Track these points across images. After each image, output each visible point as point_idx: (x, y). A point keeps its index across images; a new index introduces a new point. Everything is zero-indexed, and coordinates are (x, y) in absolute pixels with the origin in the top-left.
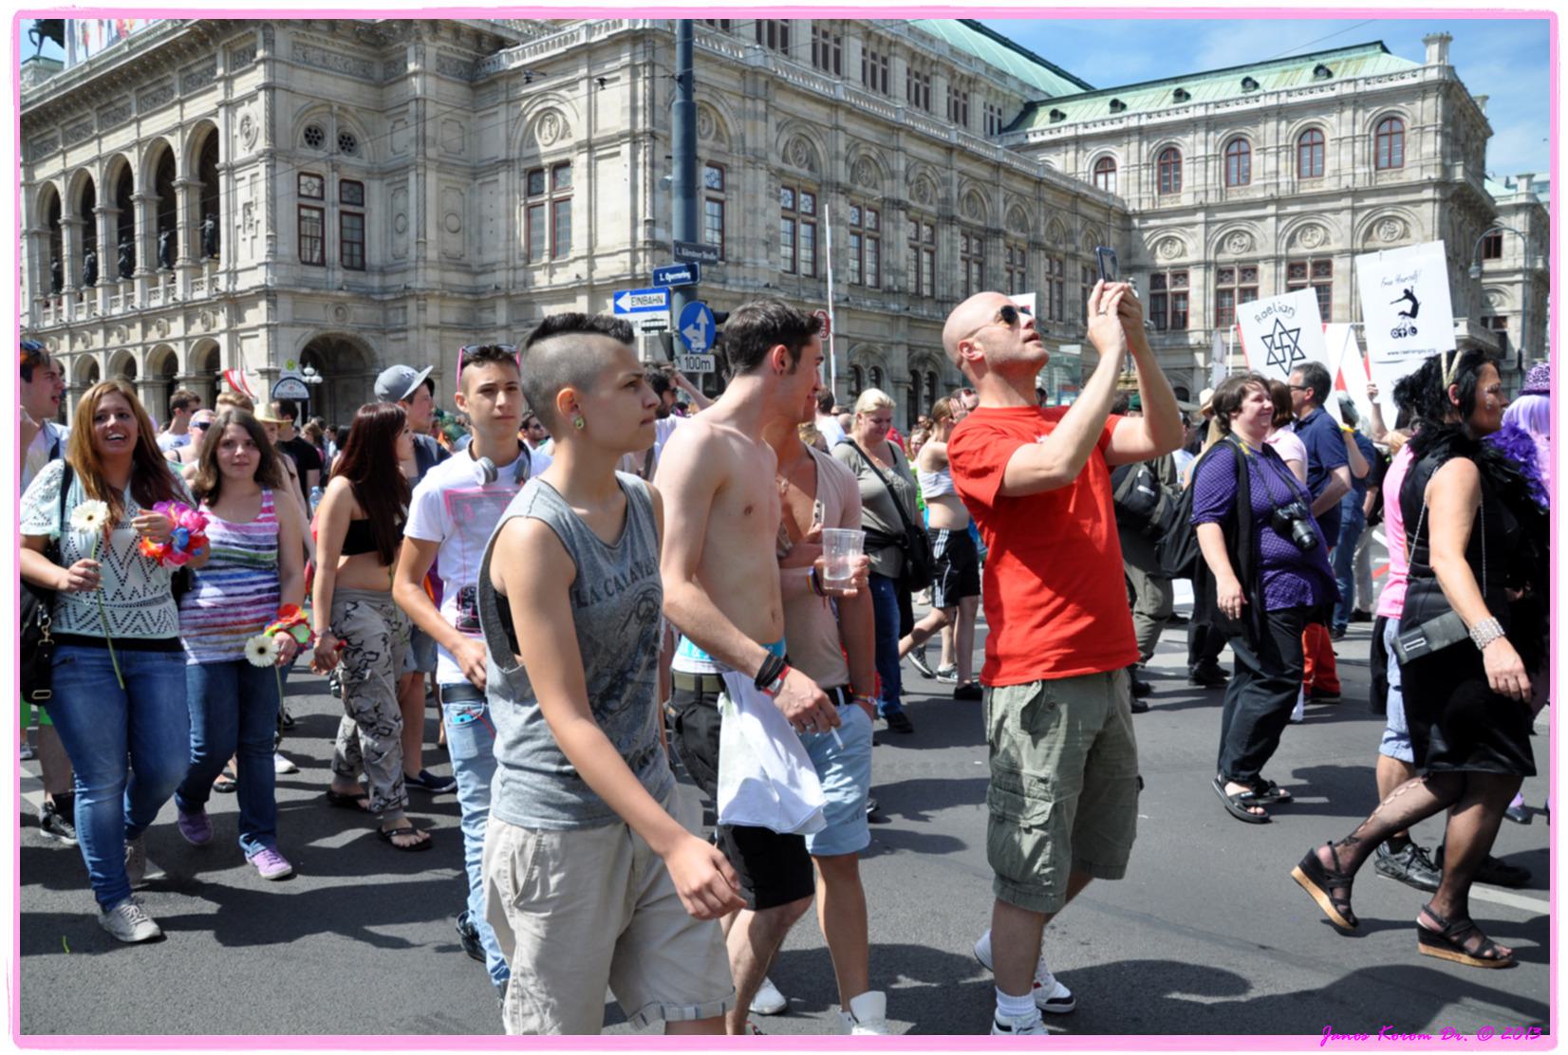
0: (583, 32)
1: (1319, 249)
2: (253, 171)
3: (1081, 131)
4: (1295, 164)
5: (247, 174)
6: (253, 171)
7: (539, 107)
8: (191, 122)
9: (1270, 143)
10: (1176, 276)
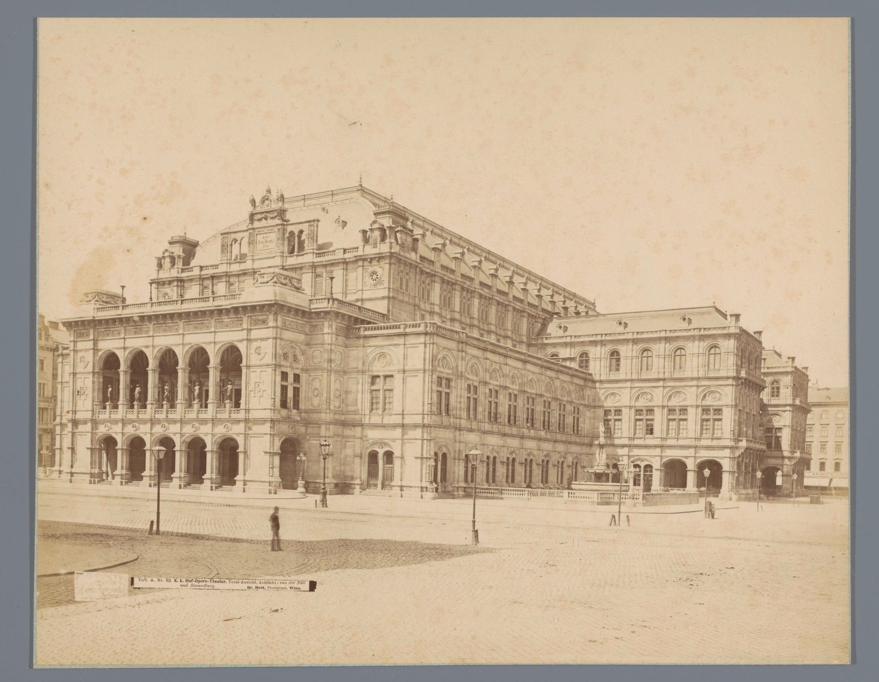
0: (402, 326)
1: (682, 404)
2: (262, 370)
3: (573, 340)
4: (672, 363)
5: (258, 370)
6: (262, 370)
7: (378, 352)
8: (221, 342)
9: (662, 353)
10: (616, 411)
